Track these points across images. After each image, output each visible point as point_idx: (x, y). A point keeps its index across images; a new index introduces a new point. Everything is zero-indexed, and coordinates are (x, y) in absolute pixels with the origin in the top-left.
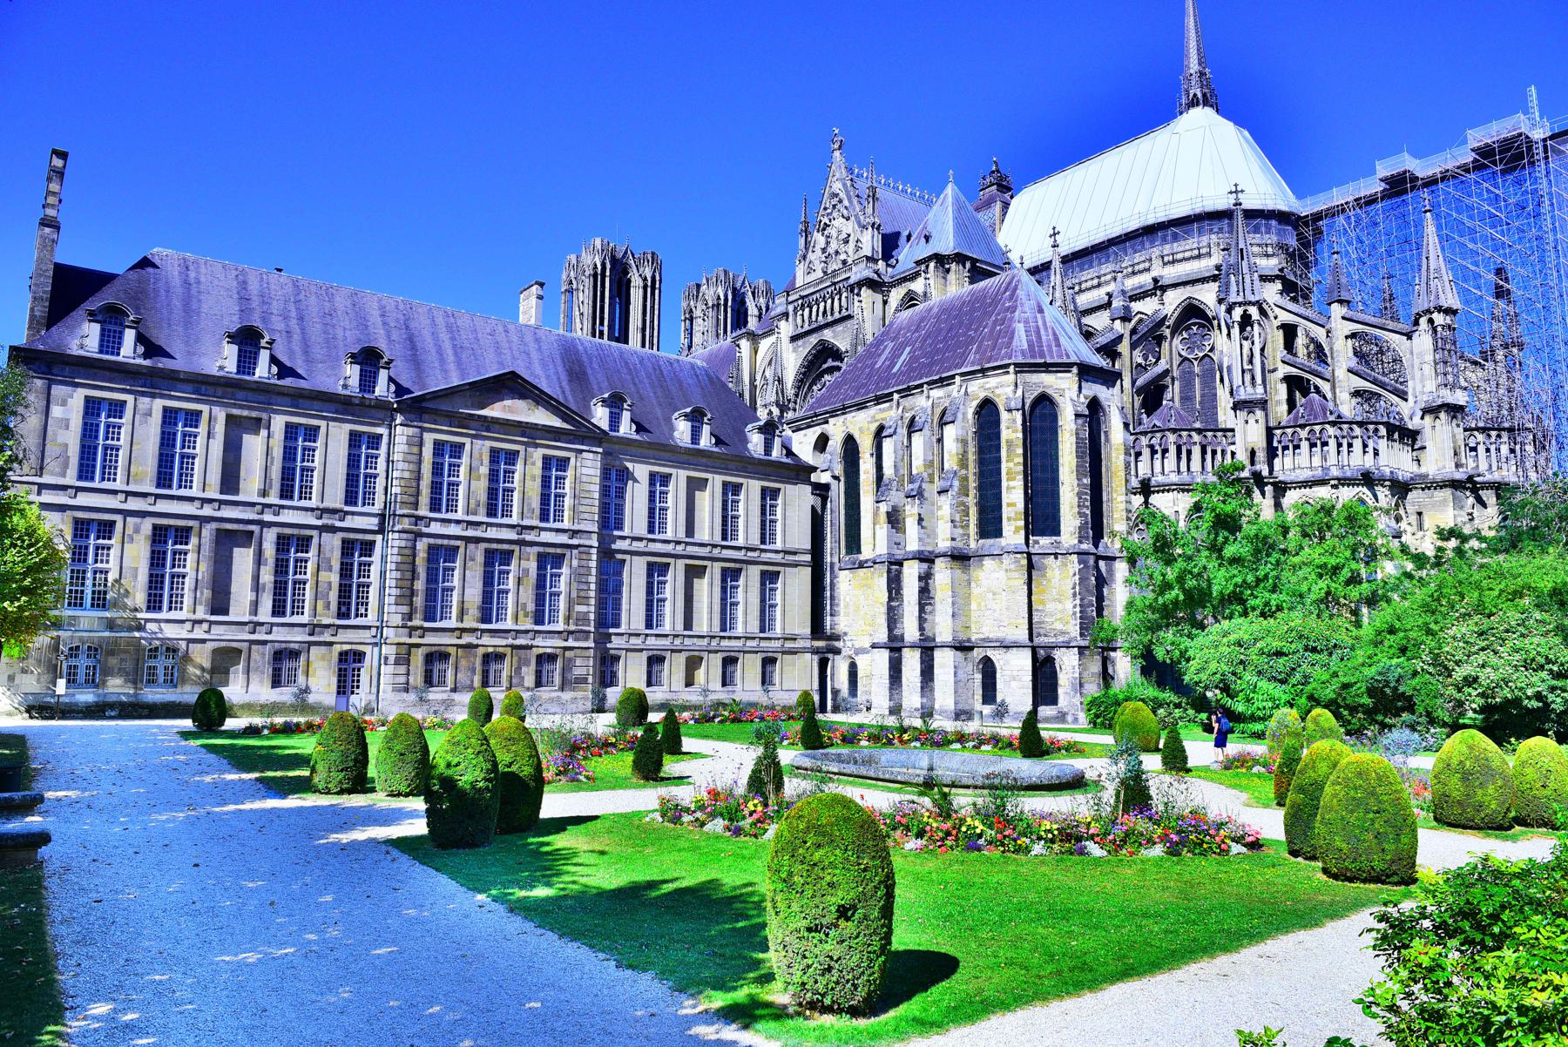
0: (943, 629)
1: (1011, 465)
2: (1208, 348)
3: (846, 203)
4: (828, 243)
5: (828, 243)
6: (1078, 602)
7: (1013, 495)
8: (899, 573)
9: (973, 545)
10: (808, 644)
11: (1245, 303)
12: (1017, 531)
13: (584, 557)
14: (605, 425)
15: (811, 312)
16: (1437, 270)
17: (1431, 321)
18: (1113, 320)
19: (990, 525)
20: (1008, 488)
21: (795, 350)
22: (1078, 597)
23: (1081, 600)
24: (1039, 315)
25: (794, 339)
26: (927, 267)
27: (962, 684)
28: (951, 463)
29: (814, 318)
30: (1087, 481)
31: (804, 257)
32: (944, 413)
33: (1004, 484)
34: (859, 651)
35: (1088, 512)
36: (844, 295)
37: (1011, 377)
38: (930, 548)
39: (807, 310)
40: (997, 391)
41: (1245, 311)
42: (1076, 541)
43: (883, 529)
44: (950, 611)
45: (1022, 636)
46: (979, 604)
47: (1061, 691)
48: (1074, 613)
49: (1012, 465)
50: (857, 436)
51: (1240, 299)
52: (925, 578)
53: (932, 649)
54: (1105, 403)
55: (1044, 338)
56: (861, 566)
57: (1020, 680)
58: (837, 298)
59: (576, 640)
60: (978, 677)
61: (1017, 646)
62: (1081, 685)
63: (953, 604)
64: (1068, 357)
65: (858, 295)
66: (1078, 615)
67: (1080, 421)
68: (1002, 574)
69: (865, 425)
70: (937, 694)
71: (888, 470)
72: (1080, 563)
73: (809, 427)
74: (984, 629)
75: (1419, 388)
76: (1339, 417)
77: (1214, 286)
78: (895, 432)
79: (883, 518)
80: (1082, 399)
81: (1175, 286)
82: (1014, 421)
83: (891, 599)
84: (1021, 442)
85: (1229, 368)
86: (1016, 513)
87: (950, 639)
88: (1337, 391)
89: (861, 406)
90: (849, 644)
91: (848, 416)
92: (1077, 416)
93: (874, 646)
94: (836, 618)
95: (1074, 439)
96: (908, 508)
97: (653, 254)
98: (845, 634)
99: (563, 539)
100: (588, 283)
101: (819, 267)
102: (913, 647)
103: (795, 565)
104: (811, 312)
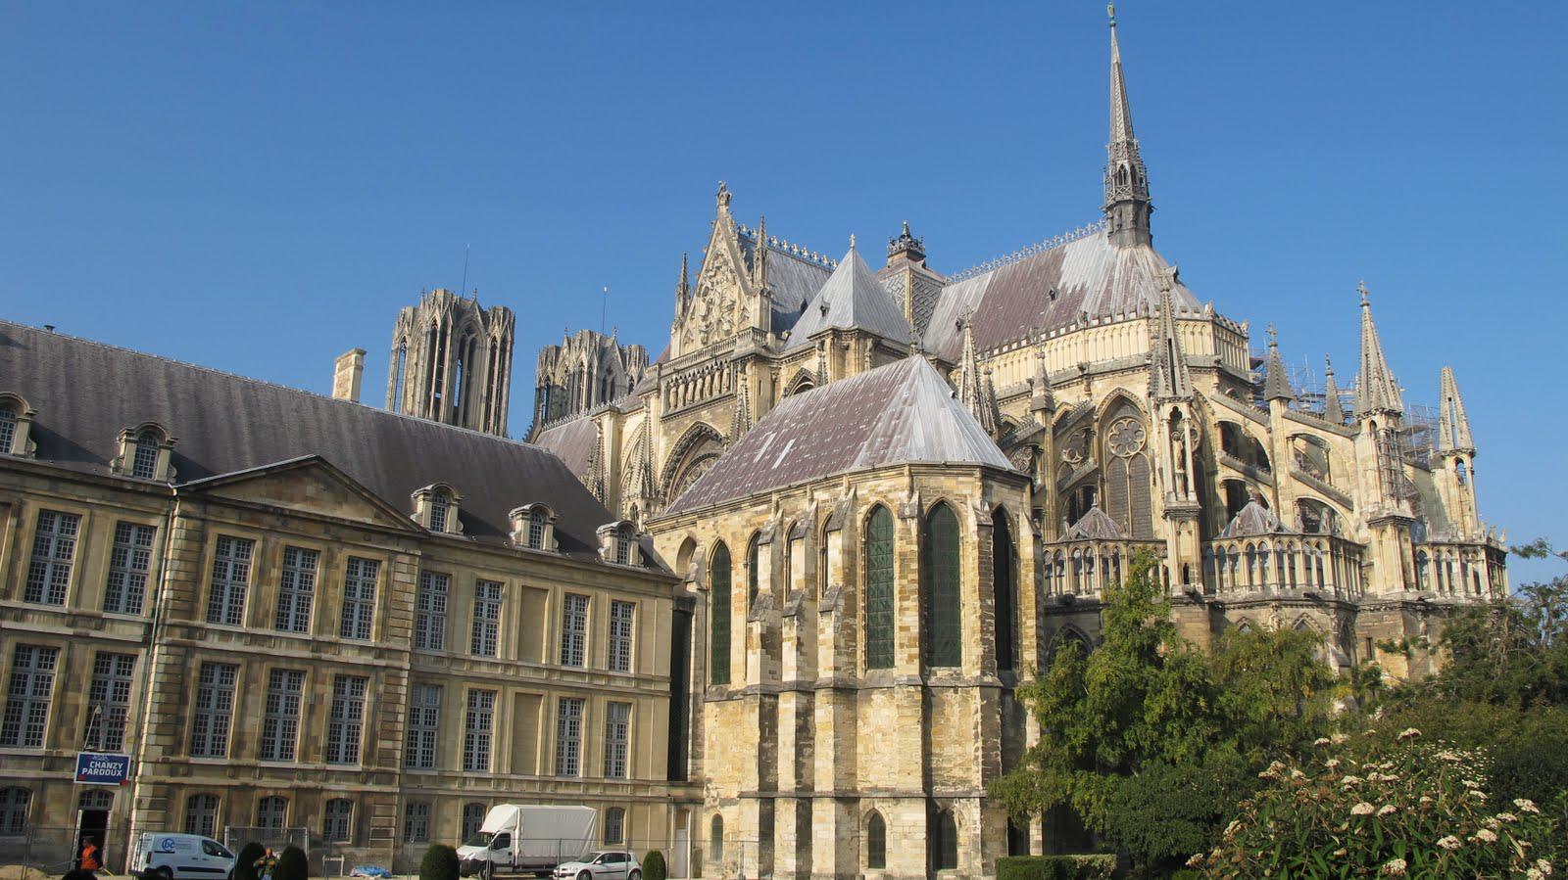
0: (824, 778)
1: (905, 582)
2: (1140, 447)
3: (732, 265)
4: (709, 310)
5: (709, 310)
6: (980, 744)
7: (907, 618)
8: (775, 707)
9: (860, 675)
10: (663, 791)
11: (1175, 399)
12: (910, 659)
13: (392, 681)
14: (425, 523)
15: (686, 389)
16: (1379, 370)
17: (1373, 423)
18: (1033, 412)
19: (880, 654)
20: (901, 609)
21: (666, 433)
22: (980, 739)
23: (984, 742)
25: (666, 419)
26: (823, 343)
27: (845, 843)
28: (835, 579)
30: (991, 602)
31: (682, 326)
32: (829, 518)
33: (897, 604)
34: (727, 802)
35: (992, 638)
36: (726, 371)
38: (809, 679)
39: (682, 388)
40: (891, 496)
41: (1175, 409)
42: (978, 673)
43: (755, 658)
45: (915, 783)
46: (866, 747)
47: (960, 851)
48: (976, 758)
49: (905, 581)
50: (729, 542)
51: (1170, 394)
52: (804, 715)
53: (810, 800)
54: (1012, 513)
56: (730, 697)
58: (717, 374)
59: (378, 783)
60: (864, 834)
61: (910, 796)
62: (983, 844)
63: (836, 746)
65: (743, 371)
66: (980, 760)
67: (983, 533)
68: (893, 712)
70: (815, 856)
71: (764, 584)
72: (982, 699)
73: (673, 528)
74: (872, 777)
75: (1364, 499)
76: (1280, 528)
77: (1144, 377)
79: (756, 640)
80: (987, 508)
82: (909, 531)
83: (762, 737)
84: (916, 557)
85: (1161, 470)
86: (910, 639)
89: (735, 508)
90: (714, 793)
91: (720, 519)
92: (980, 526)
93: (742, 796)
94: (698, 762)
95: (976, 553)
96: (785, 630)
97: (505, 310)
98: (710, 781)
99: (367, 659)
100: (425, 342)
101: (698, 337)
102: (787, 796)
103: (652, 695)
104: (686, 389)
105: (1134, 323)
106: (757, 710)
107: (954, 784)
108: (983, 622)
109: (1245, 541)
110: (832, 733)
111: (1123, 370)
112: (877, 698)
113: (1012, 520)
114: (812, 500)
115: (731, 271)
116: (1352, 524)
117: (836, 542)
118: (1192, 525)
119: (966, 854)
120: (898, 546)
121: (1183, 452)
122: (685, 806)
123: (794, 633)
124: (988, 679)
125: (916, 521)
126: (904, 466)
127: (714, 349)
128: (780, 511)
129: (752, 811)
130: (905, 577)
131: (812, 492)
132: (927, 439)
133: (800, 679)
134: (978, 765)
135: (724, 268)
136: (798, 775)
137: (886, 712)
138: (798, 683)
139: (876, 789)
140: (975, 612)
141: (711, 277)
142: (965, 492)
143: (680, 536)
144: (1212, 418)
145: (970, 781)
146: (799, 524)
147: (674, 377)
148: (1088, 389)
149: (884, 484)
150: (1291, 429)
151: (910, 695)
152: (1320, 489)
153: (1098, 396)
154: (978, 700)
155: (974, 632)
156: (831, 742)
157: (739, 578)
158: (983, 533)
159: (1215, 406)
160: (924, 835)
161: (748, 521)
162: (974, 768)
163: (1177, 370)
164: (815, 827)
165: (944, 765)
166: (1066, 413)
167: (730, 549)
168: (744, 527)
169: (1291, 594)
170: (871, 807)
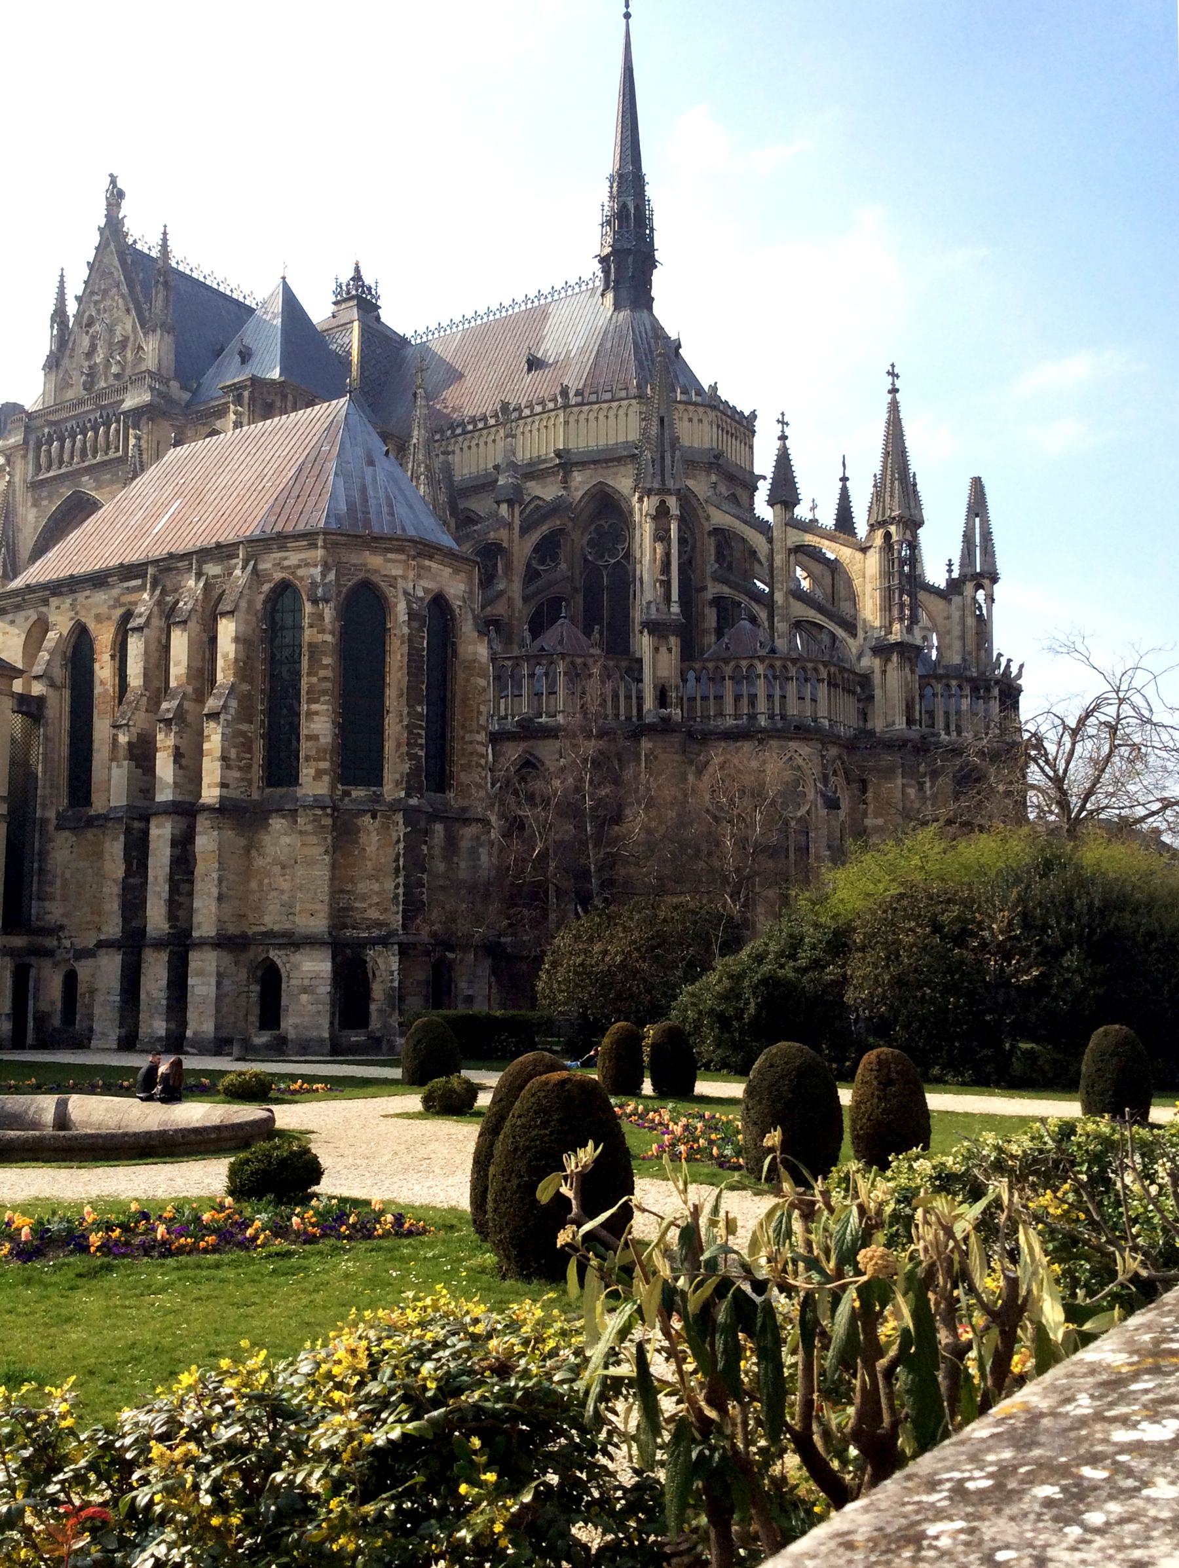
1: (314, 680)
3: (125, 289)
4: (93, 347)
5: (93, 347)
6: (401, 880)
8: (146, 833)
12: (319, 774)
15: (62, 447)
17: (888, 536)
18: (498, 503)
21: (36, 504)
22: (403, 873)
24: (369, 471)
25: (35, 486)
27: (228, 1000)
29: (66, 457)
35: (422, 753)
37: (320, 553)
38: (188, 799)
40: (300, 572)
41: (663, 502)
42: (402, 794)
44: (215, 892)
47: (373, 1007)
48: (396, 896)
50: (92, 626)
51: (656, 486)
52: (183, 845)
55: (372, 502)
56: (91, 822)
57: (313, 993)
60: (256, 988)
62: (401, 999)
63: (220, 881)
64: (404, 529)
66: (401, 899)
67: (415, 624)
69: (103, 610)
70: (191, 1015)
72: (406, 825)
73: (18, 608)
76: (773, 651)
77: (630, 470)
78: (147, 623)
79: (122, 752)
81: (583, 464)
82: (321, 617)
83: (128, 873)
86: (318, 750)
87: (213, 934)
88: (776, 619)
91: (81, 597)
92: (412, 615)
94: (47, 904)
95: (405, 648)
96: (160, 737)
98: (61, 928)
101: (79, 380)
102: (159, 945)
104: (62, 447)
105: (624, 403)
106: (122, 838)
107: (368, 928)
108: (410, 733)
109: (732, 663)
110: (216, 865)
111: (607, 461)
112: (277, 823)
113: (452, 611)
114: (199, 575)
115: (123, 296)
116: (854, 651)
117: (227, 630)
118: (673, 641)
119: (380, 1011)
120: (308, 635)
121: (668, 554)
122: (27, 960)
123: (171, 741)
124: (414, 801)
125: (332, 604)
126: (317, 534)
127: (99, 396)
128: (158, 592)
129: (110, 966)
130: (316, 674)
131: (200, 564)
132: (351, 505)
133: (179, 798)
134: (398, 905)
135: (114, 290)
136: (172, 917)
137: (286, 840)
138: (173, 803)
139: (270, 934)
140: (401, 721)
141: (96, 302)
142: (394, 572)
143: (27, 619)
144: (706, 524)
145: (387, 925)
146: (181, 604)
147: (46, 430)
148: (565, 481)
149: (293, 559)
150: (795, 539)
151: (316, 819)
152: (820, 609)
153: (577, 489)
154: (401, 827)
155: (399, 745)
156: (215, 875)
157: (104, 670)
158: (415, 624)
159: (712, 511)
160: (328, 989)
161: (117, 600)
162: (395, 909)
163: (668, 456)
164: (190, 981)
165: (357, 905)
166: (537, 507)
167: (93, 634)
168: (110, 607)
169: (780, 725)
170: (264, 956)
